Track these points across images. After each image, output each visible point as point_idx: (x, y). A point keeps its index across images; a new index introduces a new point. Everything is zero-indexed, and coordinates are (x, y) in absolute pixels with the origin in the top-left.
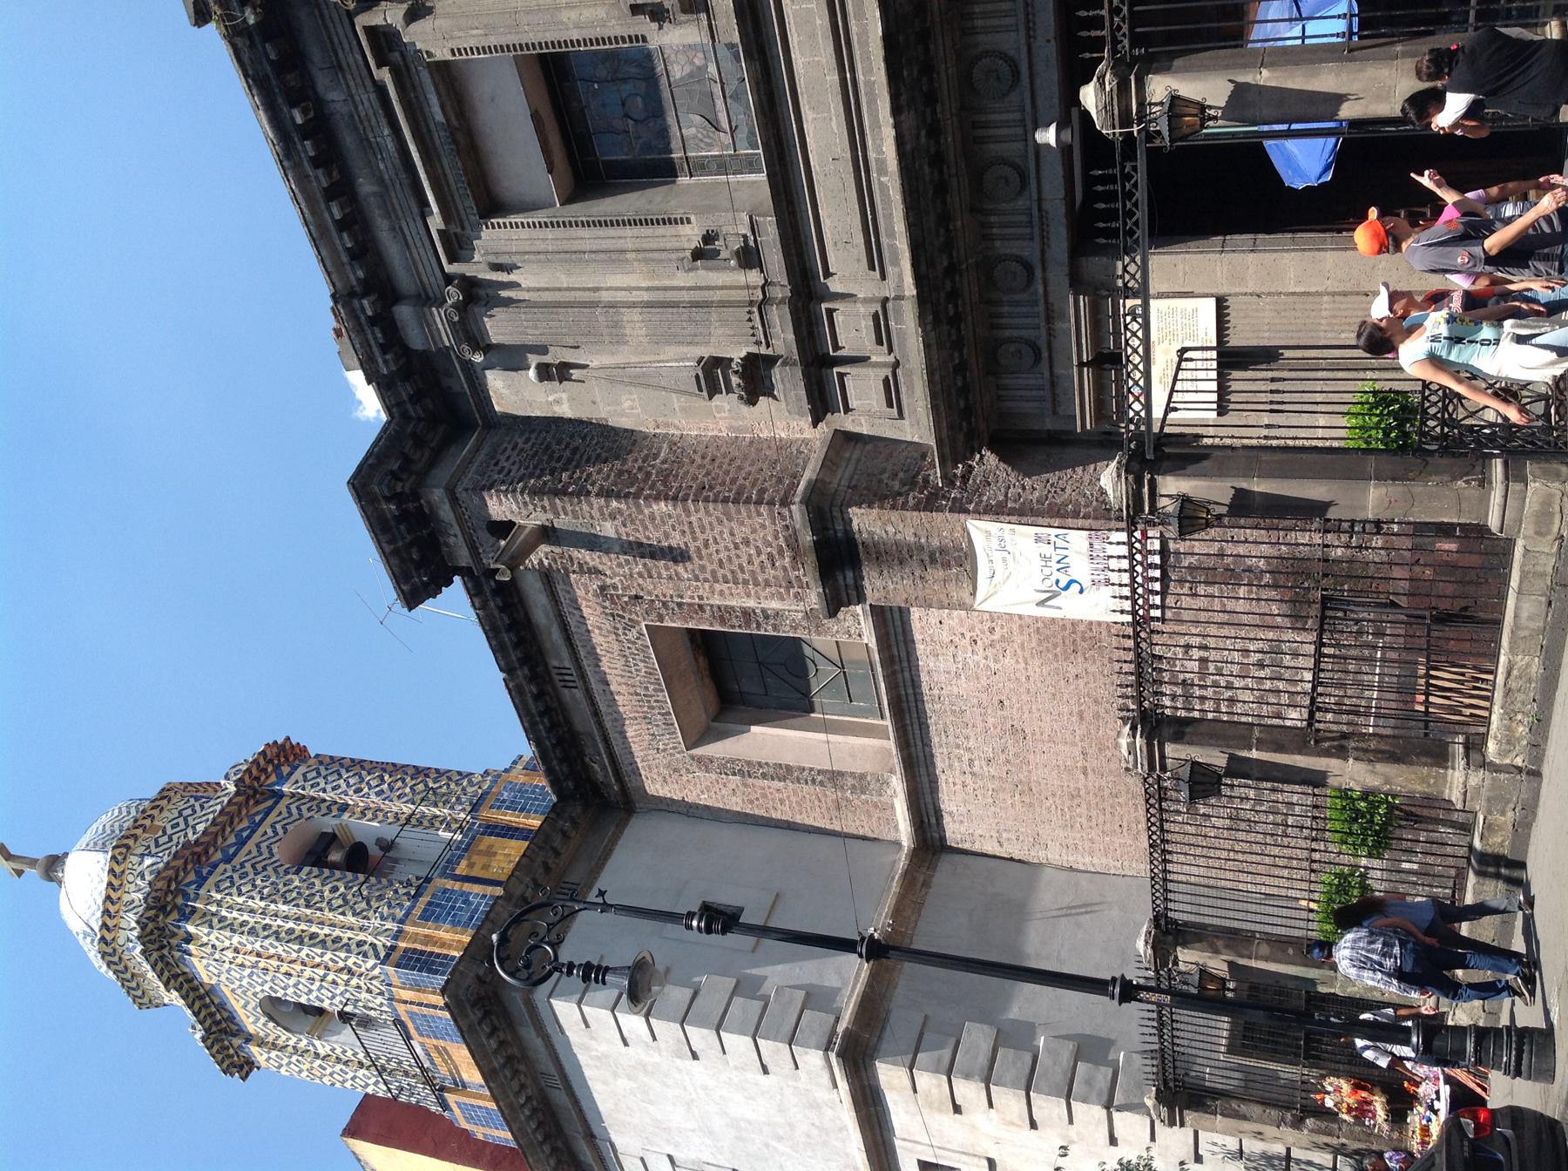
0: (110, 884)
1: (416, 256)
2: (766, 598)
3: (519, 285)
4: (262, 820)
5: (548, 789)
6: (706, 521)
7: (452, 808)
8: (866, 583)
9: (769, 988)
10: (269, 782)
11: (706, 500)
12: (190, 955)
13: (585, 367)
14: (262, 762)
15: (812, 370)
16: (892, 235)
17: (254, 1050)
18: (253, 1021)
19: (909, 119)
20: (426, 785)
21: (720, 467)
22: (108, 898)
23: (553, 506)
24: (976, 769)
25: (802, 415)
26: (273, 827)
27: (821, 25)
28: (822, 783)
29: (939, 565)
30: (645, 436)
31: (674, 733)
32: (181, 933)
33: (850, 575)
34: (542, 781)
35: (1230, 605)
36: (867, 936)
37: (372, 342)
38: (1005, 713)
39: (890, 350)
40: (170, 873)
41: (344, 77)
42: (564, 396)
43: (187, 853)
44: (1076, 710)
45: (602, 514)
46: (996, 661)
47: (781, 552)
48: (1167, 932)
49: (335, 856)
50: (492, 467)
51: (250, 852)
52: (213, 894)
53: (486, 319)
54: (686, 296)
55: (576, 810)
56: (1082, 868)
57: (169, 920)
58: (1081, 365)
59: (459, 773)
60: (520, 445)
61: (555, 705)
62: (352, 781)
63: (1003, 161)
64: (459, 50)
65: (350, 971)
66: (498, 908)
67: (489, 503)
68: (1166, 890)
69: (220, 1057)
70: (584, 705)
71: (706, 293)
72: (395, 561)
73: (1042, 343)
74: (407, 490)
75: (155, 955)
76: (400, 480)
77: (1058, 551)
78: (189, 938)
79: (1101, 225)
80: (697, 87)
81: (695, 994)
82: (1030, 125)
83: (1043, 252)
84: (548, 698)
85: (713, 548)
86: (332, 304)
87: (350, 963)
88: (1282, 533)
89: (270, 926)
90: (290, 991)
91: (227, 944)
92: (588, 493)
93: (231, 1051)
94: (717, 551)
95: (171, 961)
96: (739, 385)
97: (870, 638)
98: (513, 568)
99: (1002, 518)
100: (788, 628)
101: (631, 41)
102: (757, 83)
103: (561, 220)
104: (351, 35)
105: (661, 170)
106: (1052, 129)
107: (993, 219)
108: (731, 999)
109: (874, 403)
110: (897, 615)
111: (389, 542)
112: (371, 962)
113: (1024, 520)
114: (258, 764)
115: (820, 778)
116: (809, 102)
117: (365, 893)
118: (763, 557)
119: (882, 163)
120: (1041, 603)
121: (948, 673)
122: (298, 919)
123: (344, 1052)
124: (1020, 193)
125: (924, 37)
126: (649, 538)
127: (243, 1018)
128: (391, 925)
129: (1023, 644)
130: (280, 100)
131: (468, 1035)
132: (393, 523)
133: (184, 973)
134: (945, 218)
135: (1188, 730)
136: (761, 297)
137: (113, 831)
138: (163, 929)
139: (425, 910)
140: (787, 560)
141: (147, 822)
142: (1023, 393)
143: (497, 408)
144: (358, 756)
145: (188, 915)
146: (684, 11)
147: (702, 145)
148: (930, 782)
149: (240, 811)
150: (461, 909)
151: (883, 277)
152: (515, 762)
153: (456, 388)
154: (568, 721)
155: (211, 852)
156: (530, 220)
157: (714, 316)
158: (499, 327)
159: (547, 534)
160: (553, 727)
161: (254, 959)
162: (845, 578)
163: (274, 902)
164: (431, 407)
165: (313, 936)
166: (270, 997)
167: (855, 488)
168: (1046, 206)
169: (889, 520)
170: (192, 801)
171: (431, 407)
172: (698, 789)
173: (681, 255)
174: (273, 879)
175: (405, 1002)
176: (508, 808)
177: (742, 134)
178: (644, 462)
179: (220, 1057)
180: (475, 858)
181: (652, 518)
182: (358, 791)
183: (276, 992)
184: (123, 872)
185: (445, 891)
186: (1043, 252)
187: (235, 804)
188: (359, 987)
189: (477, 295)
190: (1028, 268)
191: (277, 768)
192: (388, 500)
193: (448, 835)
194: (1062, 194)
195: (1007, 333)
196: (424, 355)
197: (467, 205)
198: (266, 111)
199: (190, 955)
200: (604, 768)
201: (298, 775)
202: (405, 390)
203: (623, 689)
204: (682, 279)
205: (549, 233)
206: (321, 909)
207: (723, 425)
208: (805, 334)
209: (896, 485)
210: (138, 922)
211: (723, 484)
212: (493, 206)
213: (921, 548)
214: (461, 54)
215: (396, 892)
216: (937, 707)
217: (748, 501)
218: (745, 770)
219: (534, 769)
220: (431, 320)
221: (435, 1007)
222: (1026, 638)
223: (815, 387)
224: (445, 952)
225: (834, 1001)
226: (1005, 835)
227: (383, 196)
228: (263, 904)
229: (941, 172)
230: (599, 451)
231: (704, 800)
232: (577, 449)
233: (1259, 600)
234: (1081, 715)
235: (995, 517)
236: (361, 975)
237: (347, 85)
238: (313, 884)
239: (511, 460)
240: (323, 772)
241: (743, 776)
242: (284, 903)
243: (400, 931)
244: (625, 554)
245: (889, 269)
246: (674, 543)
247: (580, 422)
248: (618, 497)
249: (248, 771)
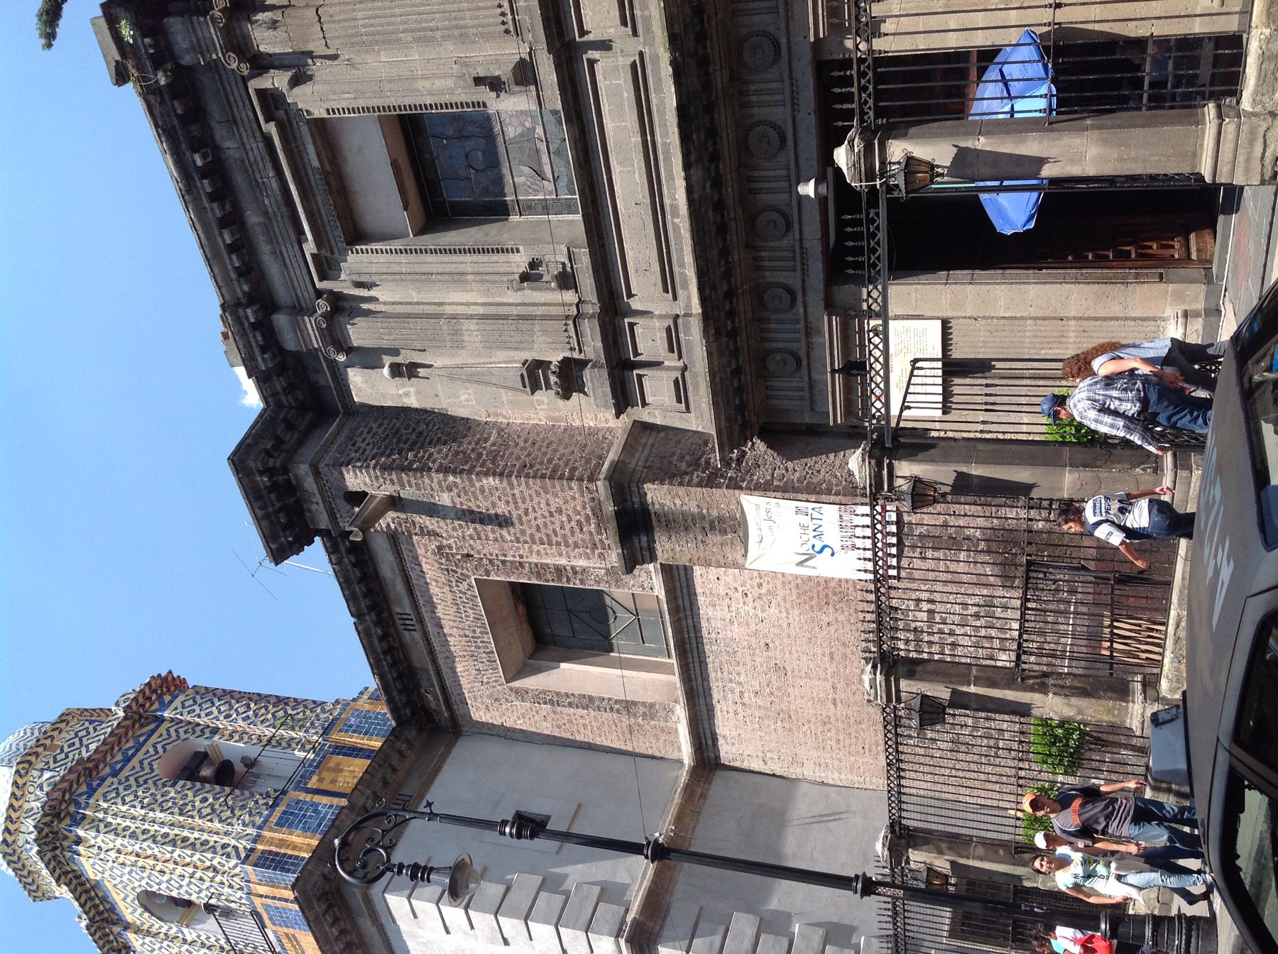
0: (13, 794)
2: (575, 557)
3: (377, 299)
4: (146, 741)
5: (389, 715)
7: (306, 731)
8: (657, 545)
9: (570, 885)
10: (153, 708)
11: (527, 476)
12: (79, 855)
13: (430, 366)
14: (147, 692)
15: (616, 371)
16: (682, 265)
17: (131, 936)
18: (130, 911)
19: (697, 173)
20: (286, 712)
21: (539, 449)
22: (11, 806)
23: (400, 479)
24: (746, 700)
25: (606, 407)
26: (155, 746)
27: (628, 98)
28: (618, 711)
29: (717, 532)
30: (478, 423)
31: (497, 668)
32: (72, 836)
33: (644, 539)
34: (383, 709)
35: (953, 567)
36: (652, 840)
37: (254, 344)
38: (770, 654)
39: (680, 357)
40: (65, 785)
41: (238, 129)
42: (412, 390)
43: (80, 768)
44: (827, 651)
45: (441, 486)
46: (763, 611)
47: (588, 519)
48: (901, 837)
49: (206, 772)
50: (350, 447)
51: (134, 768)
52: (101, 803)
53: (348, 327)
54: (514, 311)
55: (411, 733)
56: (831, 782)
57: (62, 825)
58: (833, 371)
59: (314, 702)
60: (375, 430)
61: (397, 645)
62: (223, 708)
63: (773, 208)
64: (333, 110)
65: (215, 870)
66: (342, 817)
67: (347, 476)
68: (900, 801)
69: (101, 942)
70: (421, 644)
71: (531, 308)
72: (264, 523)
73: (802, 353)
74: (278, 464)
75: (49, 855)
76: (273, 457)
77: (814, 521)
78: (79, 841)
79: (851, 259)
80: (526, 145)
81: (508, 889)
82: (793, 181)
84: (391, 639)
85: (532, 515)
86: (220, 312)
87: (215, 862)
88: (994, 509)
89: (149, 831)
90: (163, 886)
91: (111, 845)
92: (430, 469)
93: (111, 937)
94: (535, 518)
95: (63, 860)
96: (556, 383)
97: (660, 591)
98: (364, 530)
99: (769, 494)
100: (592, 582)
101: (474, 107)
102: (575, 142)
103: (413, 248)
104: (244, 95)
105: (496, 210)
106: (812, 183)
107: (763, 254)
108: (538, 893)
109: (667, 399)
110: (682, 573)
111: (262, 508)
112: (233, 862)
113: (787, 495)
114: (144, 693)
115: (616, 707)
116: (617, 158)
117: (230, 803)
118: (573, 524)
119: (675, 208)
120: (801, 563)
121: (724, 620)
122: (172, 825)
123: (208, 938)
124: (785, 235)
125: (710, 108)
126: (479, 507)
127: (123, 909)
128: (250, 830)
129: (785, 597)
130: (184, 146)
131: (314, 924)
132: (265, 492)
133: (74, 871)
134: (725, 252)
135: (919, 668)
136: (576, 312)
137: (18, 749)
138: (57, 833)
139: (280, 818)
140: (593, 526)
141: (48, 742)
142: (788, 393)
143: (356, 399)
144: (228, 687)
145: (78, 820)
146: (517, 83)
147: (530, 191)
148: (708, 710)
149: (126, 734)
150: (311, 817)
151: (675, 298)
152: (361, 693)
153: (322, 382)
154: (407, 659)
155: (100, 767)
156: (388, 247)
157: (537, 327)
158: (359, 333)
159: (395, 503)
160: (394, 664)
161: (133, 858)
162: (640, 542)
163: (153, 810)
164: (301, 397)
165: (185, 839)
166: (146, 892)
167: (649, 467)
168: (807, 245)
170: (87, 724)
171: (301, 397)
172: (516, 716)
173: (511, 277)
174: (153, 790)
175: (261, 896)
176: (354, 732)
177: (562, 183)
178: (477, 444)
179: (101, 942)
180: (324, 774)
181: (482, 490)
182: (227, 716)
183: (151, 887)
184: (25, 784)
185: (298, 802)
187: (123, 727)
188: (222, 883)
189: (342, 307)
190: (791, 293)
191: (160, 696)
192: (261, 473)
193: (302, 754)
194: (819, 235)
195: (774, 345)
196: (297, 355)
197: (336, 233)
198: (172, 155)
199: (79, 855)
200: (436, 698)
201: (177, 703)
202: (279, 384)
203: (454, 631)
204: (511, 297)
205: (403, 258)
206: (192, 817)
207: (542, 415)
208: (611, 342)
209: (683, 466)
210: (35, 827)
211: (541, 463)
212: (357, 235)
214: (334, 113)
215: (256, 802)
216: (714, 648)
217: (561, 478)
218: (555, 700)
219: (377, 699)
220: (303, 326)
221: (286, 900)
223: (619, 386)
224: (296, 853)
225: (624, 895)
226: (769, 755)
227: (267, 227)
228: (143, 812)
229: (723, 216)
230: (439, 435)
231: (520, 724)
232: (421, 433)
233: (975, 563)
234: (832, 656)
235: (762, 493)
236: (224, 873)
237: (240, 136)
238: (187, 795)
239: (367, 442)
240: (199, 701)
241: (553, 705)
242: (161, 811)
243: (259, 836)
244: (459, 519)
245: (680, 292)
246: (500, 512)
247: (425, 411)
248: (454, 473)
249: (135, 699)
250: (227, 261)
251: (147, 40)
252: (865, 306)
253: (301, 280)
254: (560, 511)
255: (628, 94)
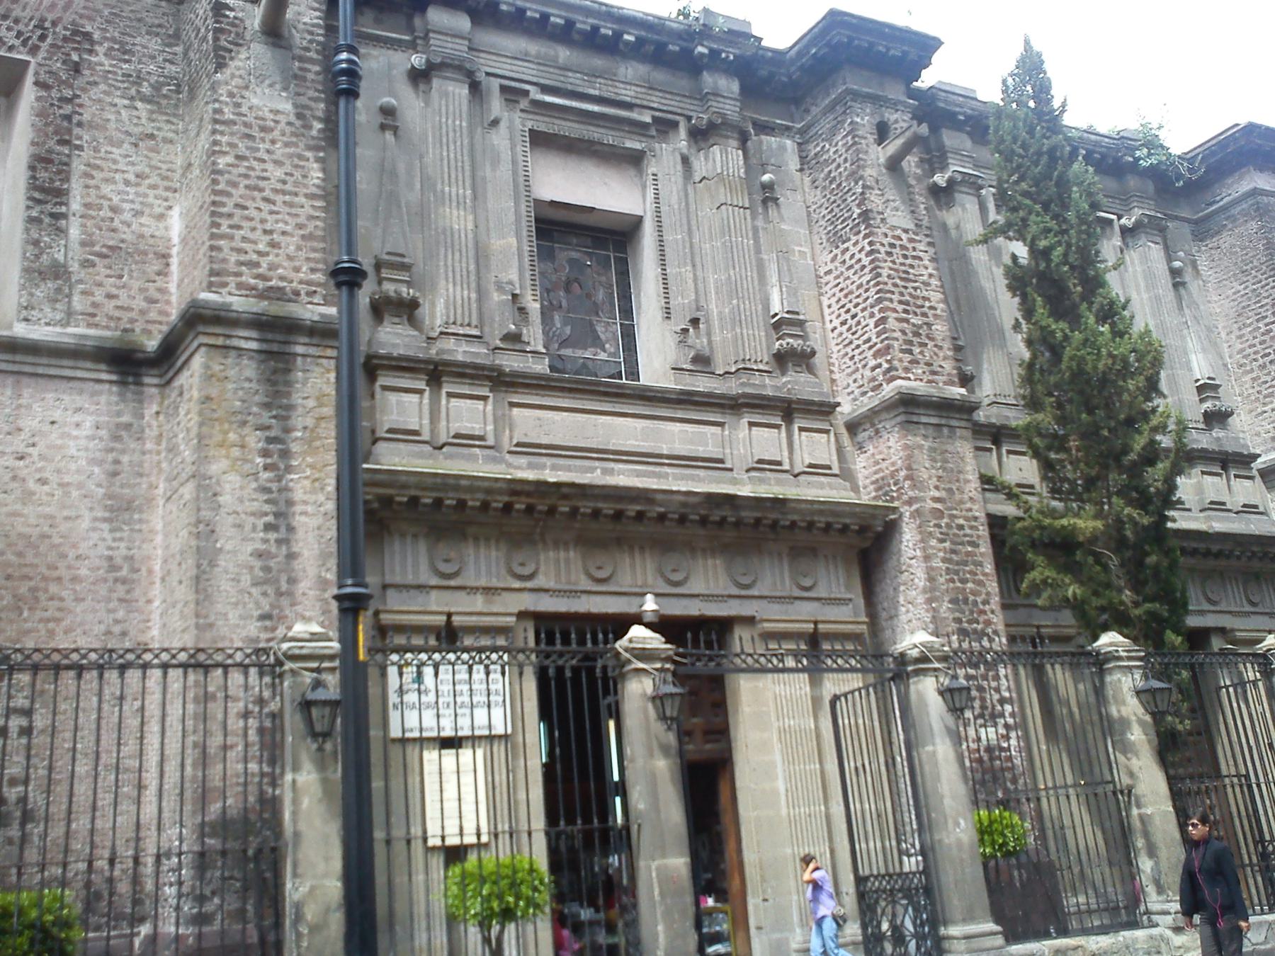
1: (504, 60)
6: (299, 211)
63: (538, 564)
83: (546, 591)
94: (259, 209)
118: (255, 257)
119: (611, 472)
140: (252, 281)
168: (584, 597)
169: (321, 405)
186: (546, 591)
190: (531, 577)
197: (543, 124)
213: (287, 430)
222: (32, 521)
245: (523, 460)
250: (534, 7)
251: (732, 57)
252: (506, 657)
253: (498, 65)
254: (273, 245)
255: (701, 451)
